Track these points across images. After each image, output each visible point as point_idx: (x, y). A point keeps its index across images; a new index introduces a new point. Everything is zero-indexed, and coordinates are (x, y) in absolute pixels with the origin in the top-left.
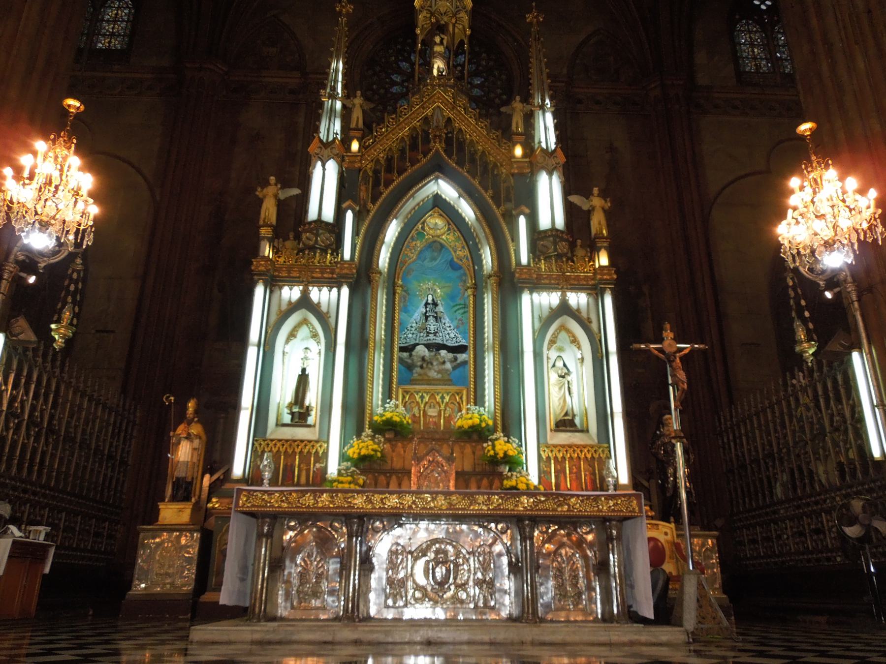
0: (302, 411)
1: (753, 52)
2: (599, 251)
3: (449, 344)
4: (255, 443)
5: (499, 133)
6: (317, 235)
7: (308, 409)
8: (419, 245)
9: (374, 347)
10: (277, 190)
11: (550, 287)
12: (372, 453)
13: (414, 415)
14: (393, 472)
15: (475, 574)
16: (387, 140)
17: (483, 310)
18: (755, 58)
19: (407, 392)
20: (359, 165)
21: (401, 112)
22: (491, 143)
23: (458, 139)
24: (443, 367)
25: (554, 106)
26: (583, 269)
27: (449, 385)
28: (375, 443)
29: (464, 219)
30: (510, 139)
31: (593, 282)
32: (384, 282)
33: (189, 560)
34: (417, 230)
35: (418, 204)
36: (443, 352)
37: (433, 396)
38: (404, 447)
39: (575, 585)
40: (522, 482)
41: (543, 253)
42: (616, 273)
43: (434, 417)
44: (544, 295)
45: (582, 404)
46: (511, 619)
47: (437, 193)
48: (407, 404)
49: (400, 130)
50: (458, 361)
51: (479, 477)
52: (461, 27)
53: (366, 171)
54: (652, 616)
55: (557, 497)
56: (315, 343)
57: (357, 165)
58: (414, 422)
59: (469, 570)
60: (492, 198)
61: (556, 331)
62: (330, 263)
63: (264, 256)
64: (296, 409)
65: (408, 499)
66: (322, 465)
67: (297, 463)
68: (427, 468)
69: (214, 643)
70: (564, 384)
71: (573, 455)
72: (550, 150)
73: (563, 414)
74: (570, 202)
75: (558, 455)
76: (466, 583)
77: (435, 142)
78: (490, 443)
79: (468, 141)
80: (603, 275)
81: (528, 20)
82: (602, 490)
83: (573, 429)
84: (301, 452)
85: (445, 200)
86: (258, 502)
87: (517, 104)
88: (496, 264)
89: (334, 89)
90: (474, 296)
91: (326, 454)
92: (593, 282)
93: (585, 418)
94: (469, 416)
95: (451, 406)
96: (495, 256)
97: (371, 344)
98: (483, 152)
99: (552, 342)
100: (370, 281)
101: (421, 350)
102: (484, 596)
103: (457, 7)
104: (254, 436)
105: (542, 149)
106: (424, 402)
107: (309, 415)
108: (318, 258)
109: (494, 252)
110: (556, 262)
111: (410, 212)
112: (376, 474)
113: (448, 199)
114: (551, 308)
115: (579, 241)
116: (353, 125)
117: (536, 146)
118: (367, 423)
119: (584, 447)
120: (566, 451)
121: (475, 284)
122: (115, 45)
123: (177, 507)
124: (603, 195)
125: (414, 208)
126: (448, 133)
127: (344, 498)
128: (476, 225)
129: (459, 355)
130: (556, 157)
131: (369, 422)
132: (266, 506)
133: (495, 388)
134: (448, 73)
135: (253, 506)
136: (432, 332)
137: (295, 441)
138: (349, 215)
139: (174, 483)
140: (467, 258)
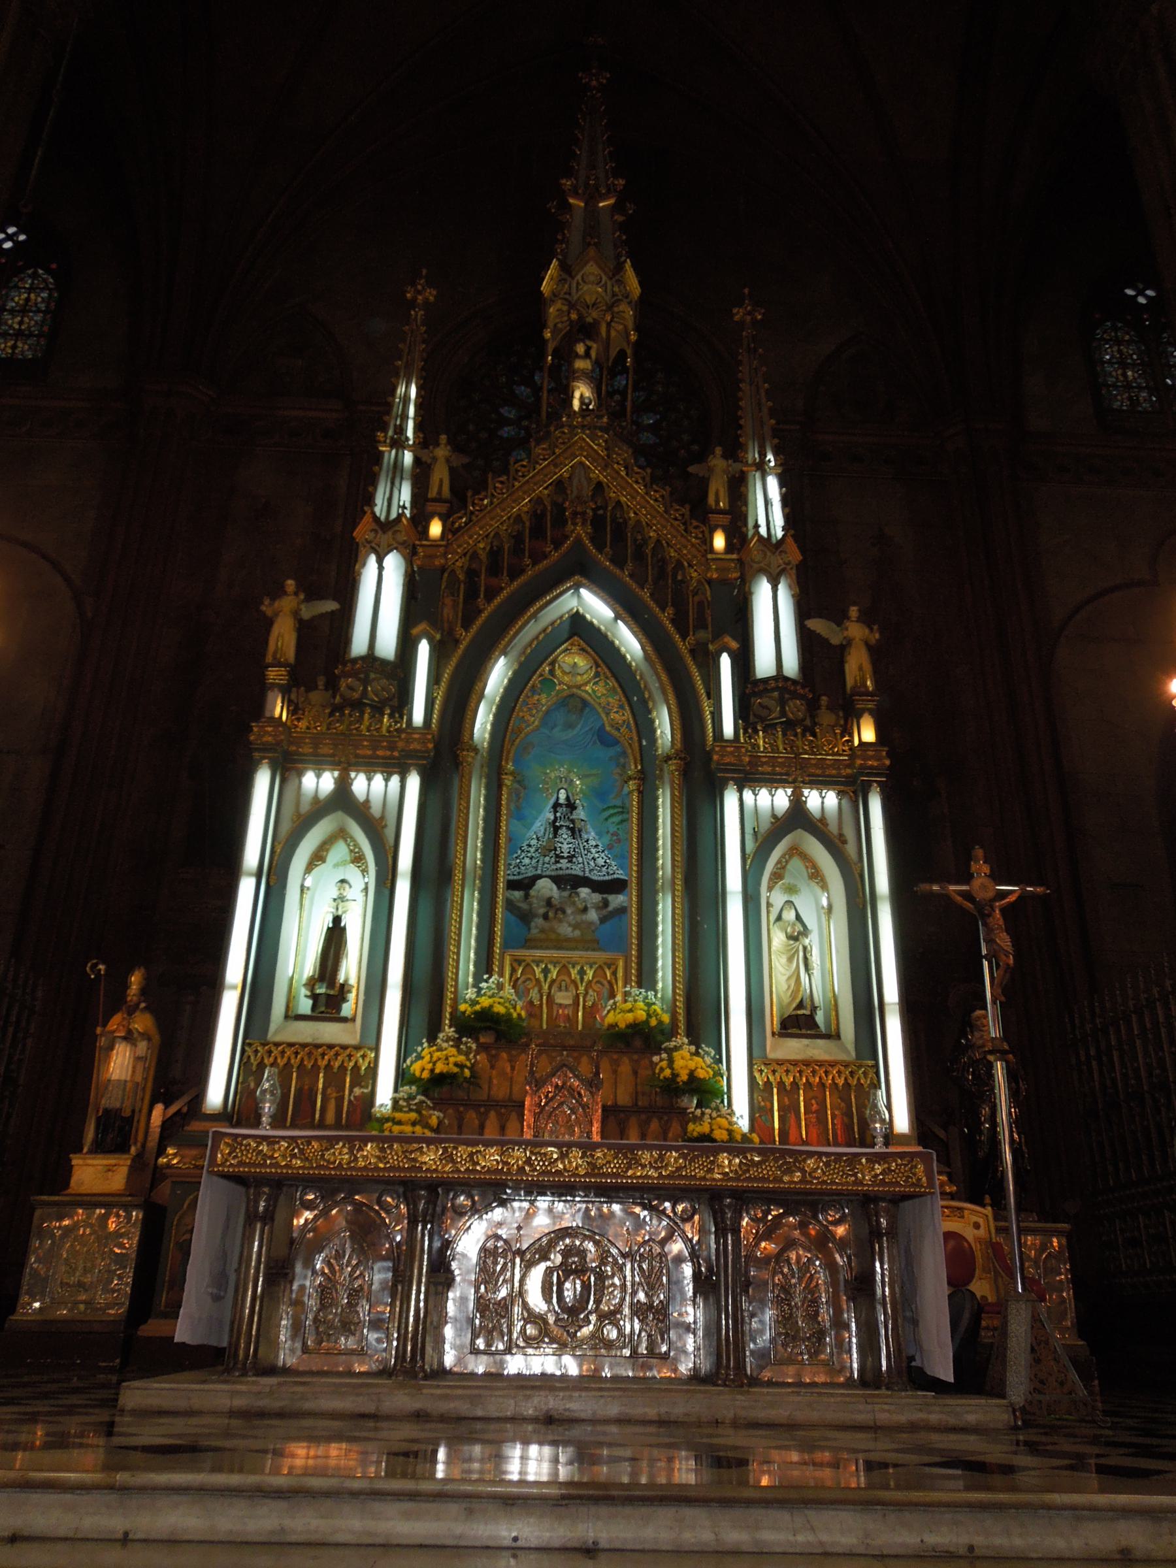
0: (332, 992)
1: (1125, 375)
2: (859, 717)
3: (595, 877)
4: (247, 1048)
5: (686, 510)
6: (366, 682)
7: (343, 991)
8: (544, 701)
9: (463, 880)
10: (298, 604)
11: (773, 781)
12: (456, 1070)
13: (531, 1003)
14: (492, 1104)
15: (634, 1293)
16: (492, 519)
17: (656, 818)
18: (1128, 386)
19: (519, 962)
20: (442, 561)
21: (517, 471)
22: (672, 525)
24: (584, 917)
25: (781, 465)
26: (830, 749)
27: (594, 950)
28: (460, 1051)
29: (624, 657)
30: (704, 520)
31: (849, 771)
32: (482, 766)
33: (120, 1260)
34: (541, 675)
35: (544, 630)
36: (584, 892)
37: (564, 970)
38: (512, 1060)
39: (813, 1317)
40: (720, 1128)
41: (762, 719)
42: (889, 755)
43: (566, 1006)
44: (764, 793)
45: (829, 987)
46: (696, 1377)
47: (578, 611)
48: (520, 982)
49: (514, 501)
50: (610, 908)
51: (643, 1117)
52: (621, 327)
53: (453, 571)
54: (950, 1379)
55: (783, 1157)
56: (358, 872)
57: (438, 562)
58: (530, 1015)
59: (624, 1286)
60: (673, 621)
61: (783, 856)
62: (389, 732)
63: (272, 718)
64: (321, 990)
65: (518, 1155)
66: (366, 1091)
67: (320, 1086)
68: (553, 1097)
69: (161, 1413)
70: (797, 951)
71: (811, 1080)
72: (774, 541)
73: (794, 1005)
74: (809, 629)
75: (784, 1079)
76: (618, 1310)
77: (575, 524)
78: (664, 1056)
79: (631, 523)
80: (865, 759)
81: (737, 318)
82: (863, 1145)
83: (812, 1032)
84: (328, 1067)
85: (591, 623)
86: (251, 1157)
87: (718, 462)
88: (678, 736)
89: (401, 430)
90: (640, 792)
91: (373, 1070)
92: (849, 771)
93: (834, 1013)
94: (629, 1005)
95: (597, 987)
96: (677, 724)
97: (458, 876)
98: (658, 541)
99: (777, 876)
100: (457, 763)
101: (545, 887)
102: (649, 1336)
103: (614, 294)
104: (245, 1037)
105: (760, 537)
106: (549, 980)
107: (344, 1000)
108: (366, 722)
109: (675, 715)
110: (784, 735)
111: (530, 644)
112: (461, 1109)
113: (595, 622)
114: (774, 816)
115: (824, 700)
116: (433, 493)
117: (751, 533)
118: (448, 1016)
119: (832, 1064)
120: (800, 1072)
121: (642, 772)
122: (22, 352)
123: (105, 1162)
124: (866, 619)
125: (537, 637)
126: (598, 508)
127: (403, 1152)
128: (645, 667)
129: (611, 898)
130: (781, 552)
131: (451, 1014)
132: (264, 1165)
133: (674, 957)
134: (599, 406)
135: (241, 1164)
136: (566, 855)
137: (317, 1046)
138: (424, 649)
139: (98, 1119)
140: (628, 726)
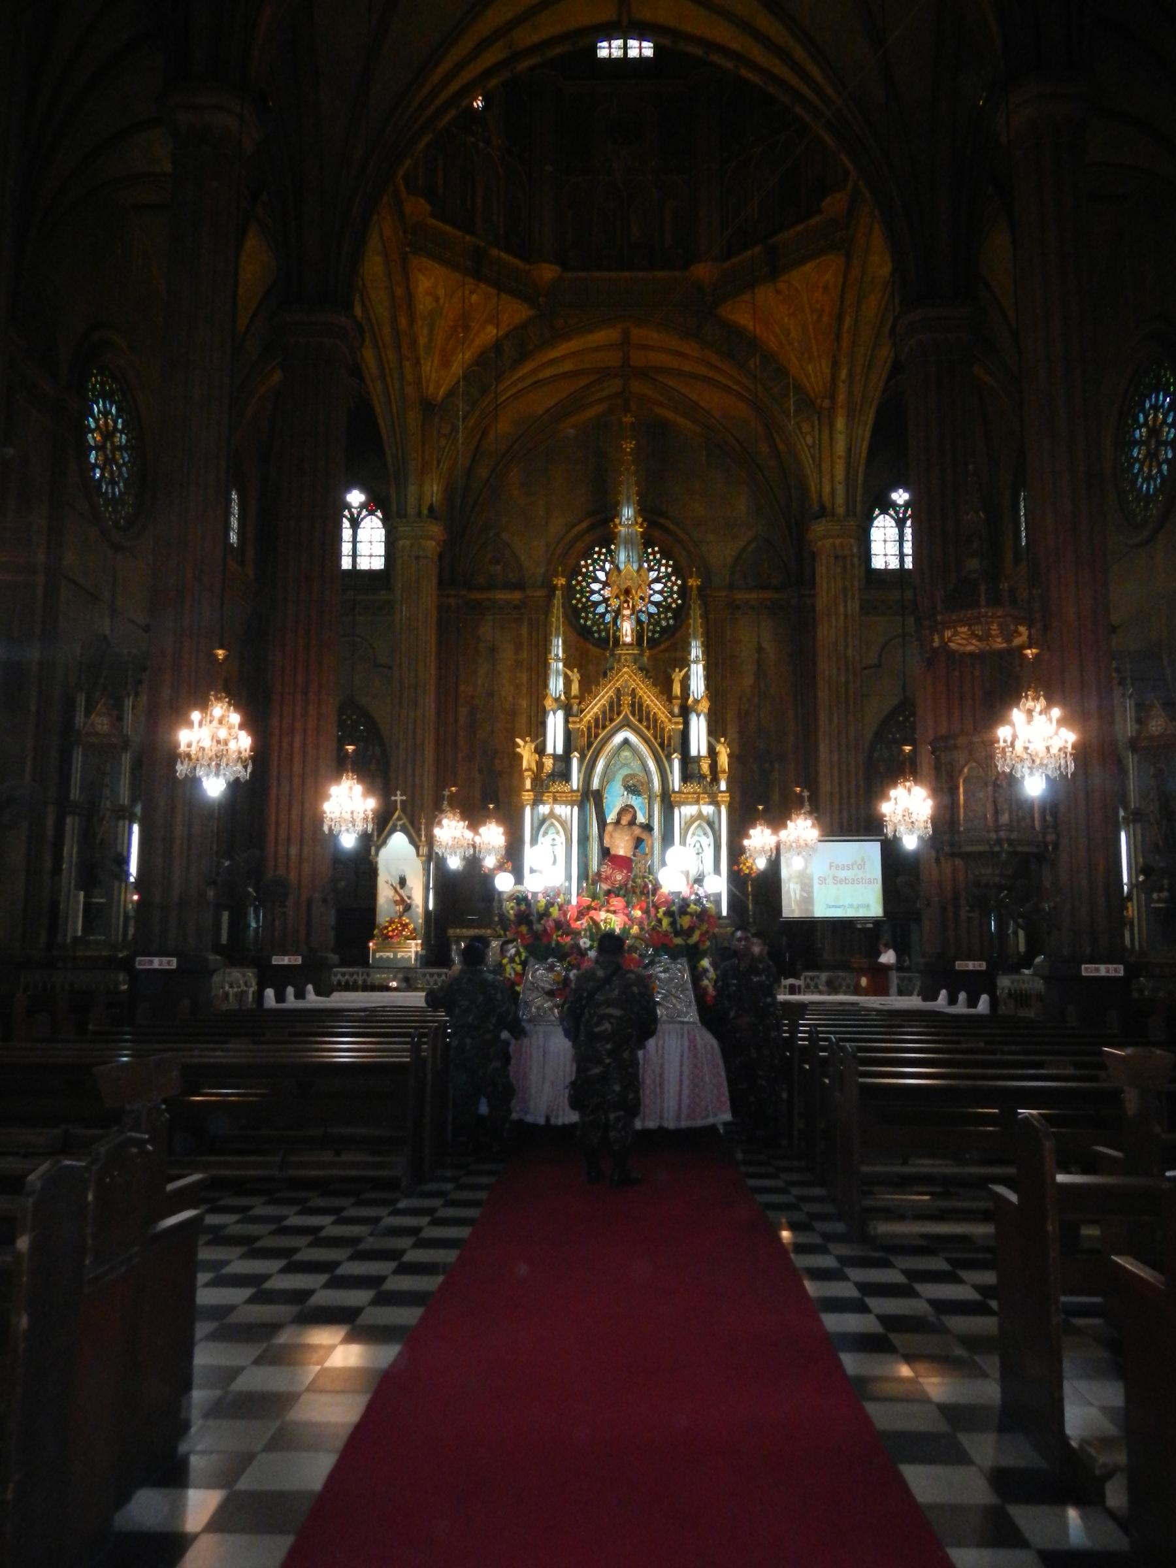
11: (691, 804)
23: (638, 702)
44: (688, 807)
72: (700, 698)
81: (690, 584)
88: (660, 789)
89: (557, 655)
90: (649, 803)
97: (591, 839)
99: (693, 834)
117: (691, 695)
